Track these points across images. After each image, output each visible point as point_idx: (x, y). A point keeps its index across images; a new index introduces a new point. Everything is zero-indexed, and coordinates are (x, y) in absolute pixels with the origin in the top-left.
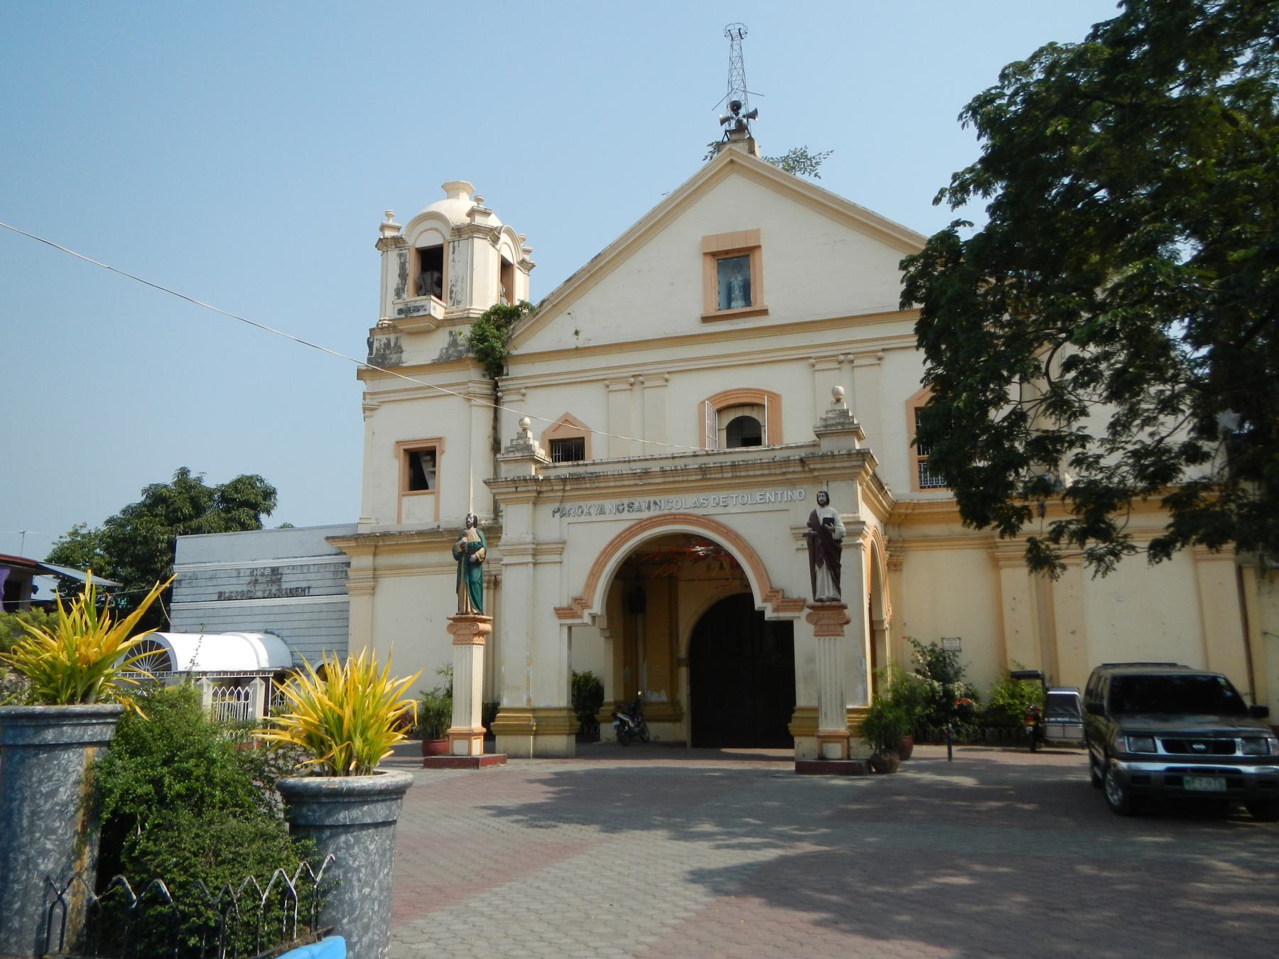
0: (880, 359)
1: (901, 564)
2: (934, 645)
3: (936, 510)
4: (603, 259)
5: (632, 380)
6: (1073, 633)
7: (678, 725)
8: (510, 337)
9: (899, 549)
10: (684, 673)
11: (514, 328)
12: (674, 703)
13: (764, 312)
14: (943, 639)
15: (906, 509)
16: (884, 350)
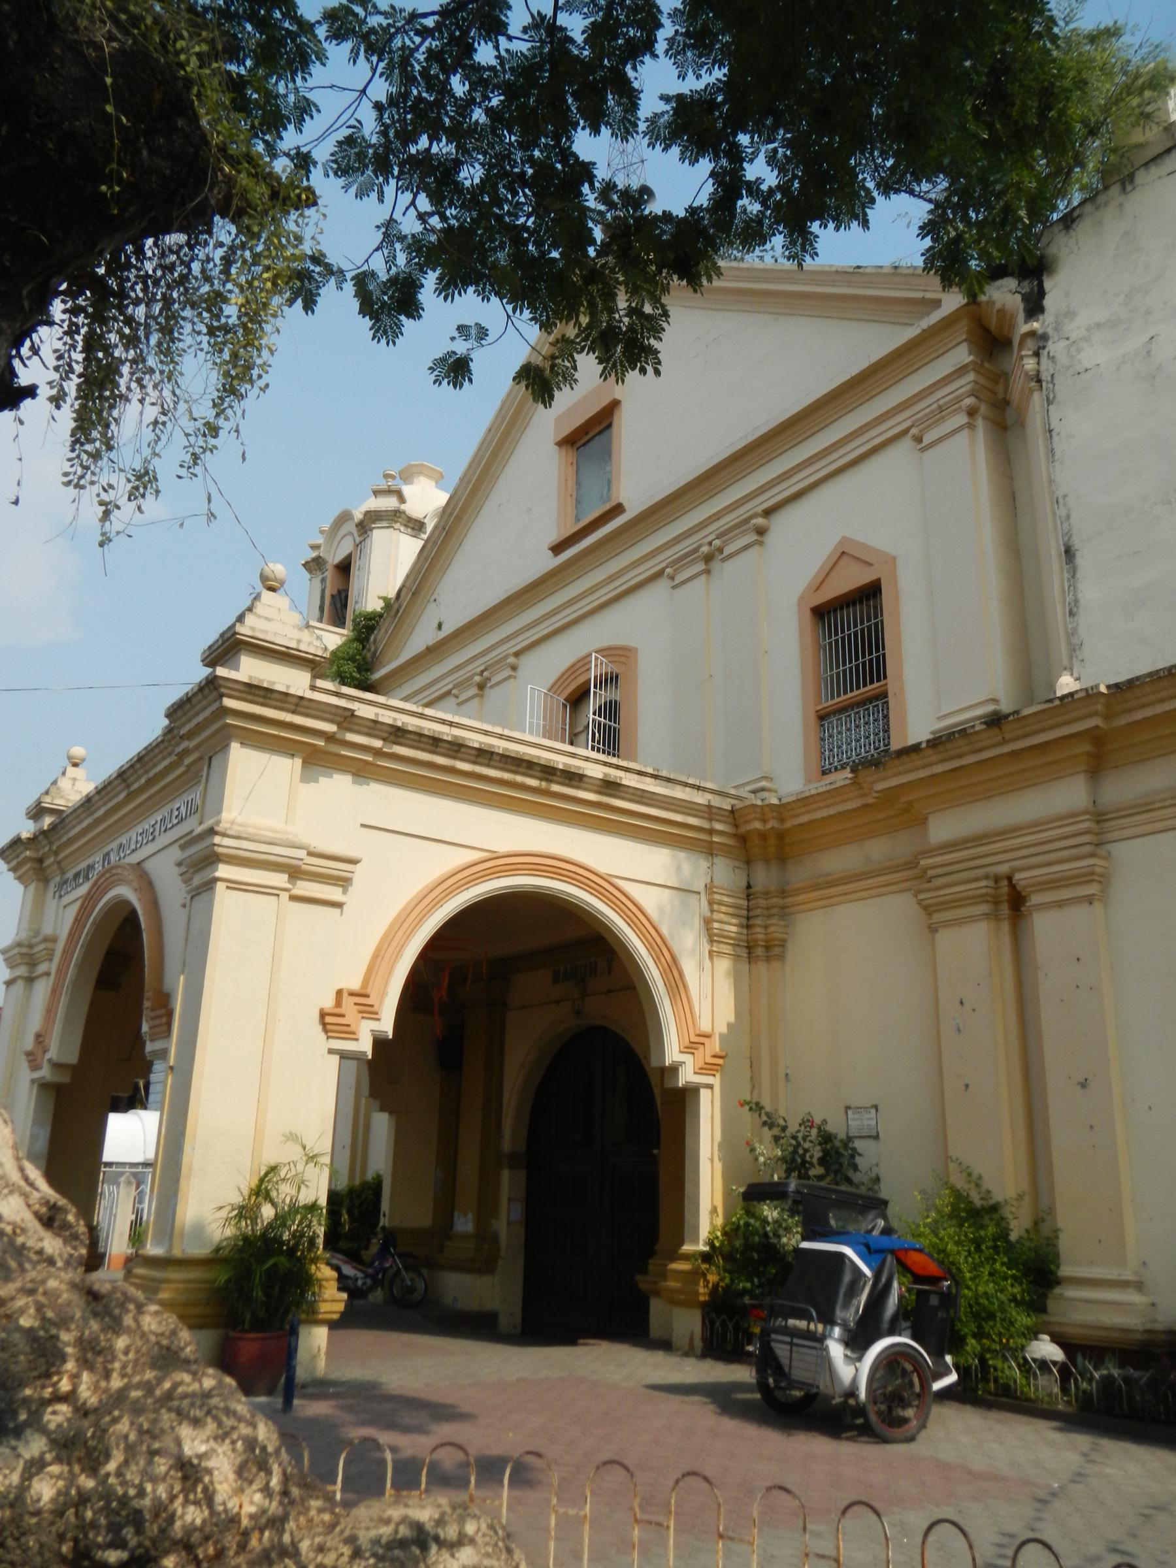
0: (761, 531)
1: (783, 944)
2: (825, 1122)
3: (819, 815)
4: (456, 505)
5: (477, 679)
6: (1083, 1085)
7: (487, 1280)
8: (374, 654)
9: (775, 911)
10: (509, 1183)
11: (375, 640)
12: (484, 1236)
13: (618, 509)
14: (847, 1108)
15: (764, 821)
16: (768, 513)
